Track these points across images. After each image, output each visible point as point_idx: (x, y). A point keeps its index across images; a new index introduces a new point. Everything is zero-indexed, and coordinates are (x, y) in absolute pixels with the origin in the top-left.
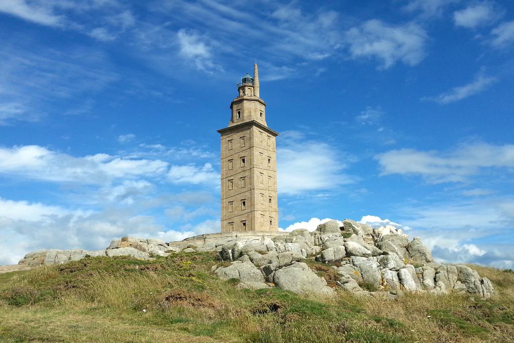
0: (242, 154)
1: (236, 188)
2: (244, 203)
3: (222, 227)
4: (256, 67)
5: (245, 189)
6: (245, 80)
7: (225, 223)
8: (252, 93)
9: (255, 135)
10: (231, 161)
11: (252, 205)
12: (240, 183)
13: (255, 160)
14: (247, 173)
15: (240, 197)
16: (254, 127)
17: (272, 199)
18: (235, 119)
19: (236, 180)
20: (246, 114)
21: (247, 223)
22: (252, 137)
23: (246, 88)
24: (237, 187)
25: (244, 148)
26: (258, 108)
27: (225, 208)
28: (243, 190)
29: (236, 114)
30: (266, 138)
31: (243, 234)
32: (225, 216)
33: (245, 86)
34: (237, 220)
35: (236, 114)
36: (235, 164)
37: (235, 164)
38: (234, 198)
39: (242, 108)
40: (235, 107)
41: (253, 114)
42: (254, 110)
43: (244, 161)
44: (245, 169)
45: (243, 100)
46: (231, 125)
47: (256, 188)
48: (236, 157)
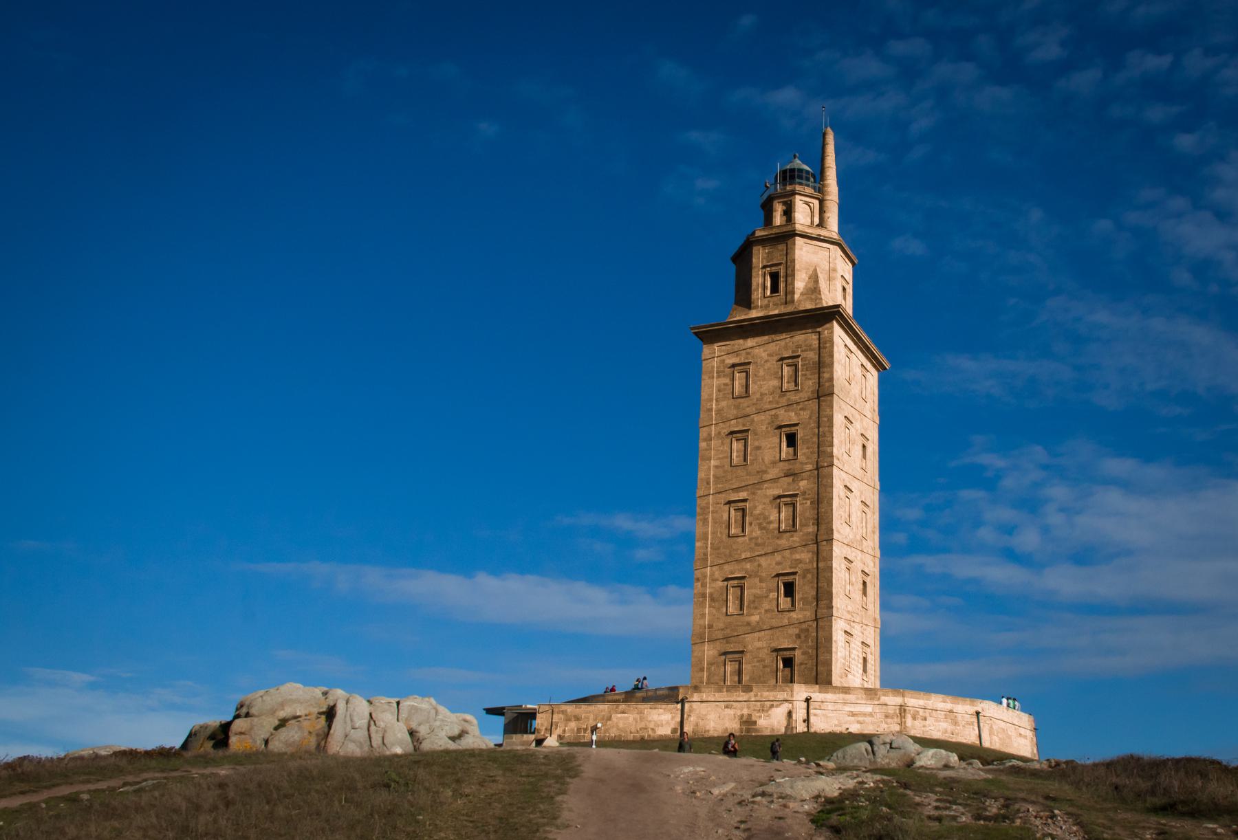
1: (757, 533)
2: (789, 590)
4: (830, 139)
5: (796, 538)
9: (836, 355)
11: (823, 597)
12: (773, 516)
13: (835, 441)
15: (770, 565)
16: (839, 335)
17: (868, 580)
18: (757, 295)
19: (760, 505)
20: (800, 284)
21: (798, 656)
22: (827, 360)
24: (762, 528)
25: (794, 397)
26: (839, 268)
27: (712, 600)
28: (784, 542)
29: (760, 281)
30: (858, 371)
31: (829, 696)
32: (710, 626)
33: (794, 193)
34: (758, 644)
36: (758, 448)
40: (760, 256)
41: (823, 284)
44: (796, 467)
45: (793, 234)
46: (741, 315)
47: (836, 535)
48: (761, 422)
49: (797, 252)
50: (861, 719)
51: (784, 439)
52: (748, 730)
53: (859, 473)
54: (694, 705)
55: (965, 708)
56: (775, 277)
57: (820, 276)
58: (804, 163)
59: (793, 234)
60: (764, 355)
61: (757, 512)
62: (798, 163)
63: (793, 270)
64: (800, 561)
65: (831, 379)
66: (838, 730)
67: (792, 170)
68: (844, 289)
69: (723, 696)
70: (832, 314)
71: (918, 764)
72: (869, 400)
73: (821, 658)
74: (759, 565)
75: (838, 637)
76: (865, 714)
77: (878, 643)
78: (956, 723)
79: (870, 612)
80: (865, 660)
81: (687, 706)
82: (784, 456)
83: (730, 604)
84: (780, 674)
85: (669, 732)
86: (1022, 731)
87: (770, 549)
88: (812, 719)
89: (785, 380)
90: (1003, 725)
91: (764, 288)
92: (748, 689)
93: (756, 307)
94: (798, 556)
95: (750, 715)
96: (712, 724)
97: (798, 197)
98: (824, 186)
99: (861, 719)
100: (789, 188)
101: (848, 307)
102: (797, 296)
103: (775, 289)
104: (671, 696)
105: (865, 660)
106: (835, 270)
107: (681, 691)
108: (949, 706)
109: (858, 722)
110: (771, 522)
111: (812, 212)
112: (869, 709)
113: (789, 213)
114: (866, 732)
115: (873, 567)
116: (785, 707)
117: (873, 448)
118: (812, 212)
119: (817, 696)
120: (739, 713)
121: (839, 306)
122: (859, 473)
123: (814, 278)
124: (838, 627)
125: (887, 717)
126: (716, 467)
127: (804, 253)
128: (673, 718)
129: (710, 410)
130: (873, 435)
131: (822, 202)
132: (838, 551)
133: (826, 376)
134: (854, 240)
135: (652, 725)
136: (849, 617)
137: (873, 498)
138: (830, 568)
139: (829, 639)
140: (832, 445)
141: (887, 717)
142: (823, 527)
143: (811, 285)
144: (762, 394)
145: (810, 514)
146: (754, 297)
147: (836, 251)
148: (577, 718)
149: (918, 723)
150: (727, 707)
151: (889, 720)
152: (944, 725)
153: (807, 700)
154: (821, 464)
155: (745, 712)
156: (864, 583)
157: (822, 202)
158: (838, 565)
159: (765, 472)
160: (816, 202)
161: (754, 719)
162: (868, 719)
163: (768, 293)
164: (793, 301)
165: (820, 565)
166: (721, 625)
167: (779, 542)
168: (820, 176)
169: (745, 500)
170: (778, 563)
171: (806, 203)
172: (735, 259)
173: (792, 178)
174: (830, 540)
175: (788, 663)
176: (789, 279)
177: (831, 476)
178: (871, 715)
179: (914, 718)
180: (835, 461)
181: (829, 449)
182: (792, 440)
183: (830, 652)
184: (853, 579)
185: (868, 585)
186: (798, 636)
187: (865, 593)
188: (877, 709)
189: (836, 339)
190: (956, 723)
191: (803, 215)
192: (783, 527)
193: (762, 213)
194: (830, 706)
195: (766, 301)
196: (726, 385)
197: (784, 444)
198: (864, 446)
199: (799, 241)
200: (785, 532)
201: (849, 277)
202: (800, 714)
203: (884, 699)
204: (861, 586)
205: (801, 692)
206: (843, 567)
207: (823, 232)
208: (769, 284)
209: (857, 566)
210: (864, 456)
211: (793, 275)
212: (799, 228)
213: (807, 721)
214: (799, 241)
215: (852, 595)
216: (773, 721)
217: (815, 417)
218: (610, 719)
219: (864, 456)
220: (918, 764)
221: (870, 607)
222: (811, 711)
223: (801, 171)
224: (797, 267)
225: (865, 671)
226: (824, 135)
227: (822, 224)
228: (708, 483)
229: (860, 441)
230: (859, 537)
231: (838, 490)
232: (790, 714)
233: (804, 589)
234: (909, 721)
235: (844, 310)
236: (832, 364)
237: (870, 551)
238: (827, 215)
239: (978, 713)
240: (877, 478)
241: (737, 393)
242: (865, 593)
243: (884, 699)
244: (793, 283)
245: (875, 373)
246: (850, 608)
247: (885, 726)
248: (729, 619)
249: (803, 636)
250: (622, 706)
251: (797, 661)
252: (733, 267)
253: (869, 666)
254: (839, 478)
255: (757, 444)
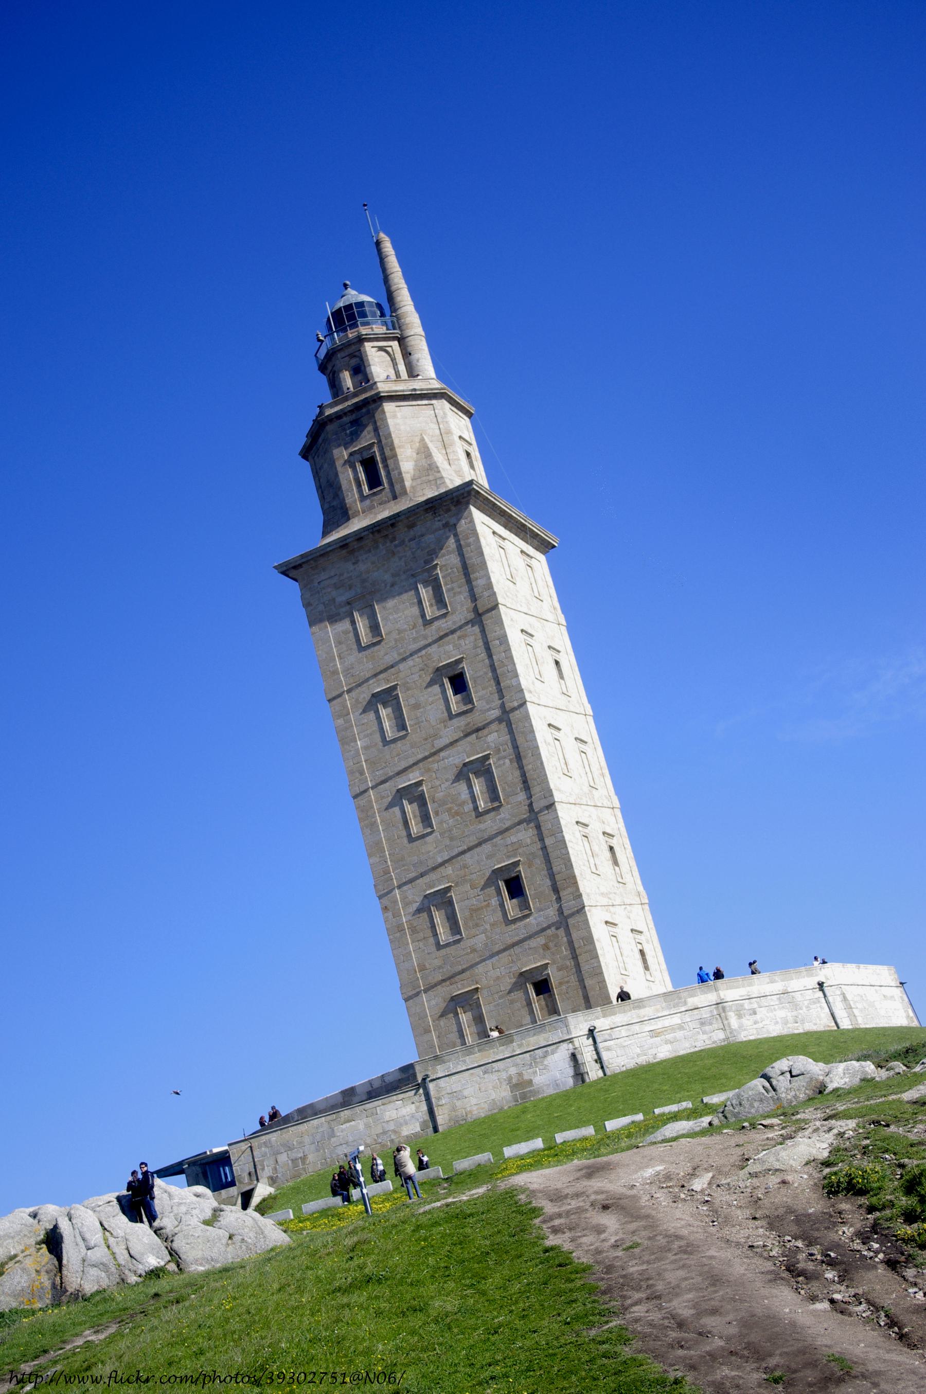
0: (446, 654)
2: (515, 887)
3: (420, 1029)
4: (388, 247)
5: (506, 816)
6: (347, 317)
7: (431, 1003)
8: (402, 368)
9: (486, 551)
10: (388, 697)
13: (520, 669)
14: (495, 737)
17: (614, 842)
18: (352, 496)
20: (407, 465)
23: (369, 348)
24: (453, 815)
25: (444, 625)
28: (490, 824)
30: (519, 562)
32: (422, 968)
33: (361, 340)
35: (350, 479)
36: (417, 706)
37: (417, 706)
38: (449, 870)
39: (383, 440)
41: (439, 458)
42: (432, 442)
43: (459, 684)
44: (476, 719)
45: (378, 399)
47: (557, 796)
49: (390, 422)
50: (669, 1037)
51: (448, 685)
52: (524, 1096)
53: (562, 702)
54: (442, 1082)
55: (802, 983)
56: (370, 466)
57: (430, 445)
58: (360, 293)
59: (378, 399)
60: (387, 577)
61: (440, 795)
62: (353, 296)
63: (393, 448)
64: (520, 844)
65: (489, 586)
66: (642, 1060)
67: (349, 307)
68: (468, 454)
69: (477, 1058)
70: (464, 496)
71: (831, 1087)
72: (545, 597)
73: (585, 968)
74: (465, 867)
75: (599, 932)
76: (672, 1029)
77: (651, 925)
78: (795, 1006)
79: (630, 886)
80: (642, 952)
81: (431, 1086)
82: (454, 708)
83: (440, 930)
84: (536, 1006)
85: (418, 1129)
86: (884, 990)
87: (473, 841)
88: (605, 1056)
89: (426, 604)
90: (860, 990)
91: (359, 485)
92: (505, 1038)
93: (356, 514)
94: (514, 839)
95: (520, 1074)
96: (474, 1101)
97: (368, 345)
98: (398, 318)
99: (669, 1037)
100: (351, 334)
101: (482, 479)
102: (408, 484)
103: (374, 481)
104: (406, 1079)
105: (642, 952)
106: (449, 432)
107: (418, 1068)
108: (778, 987)
109: (667, 1042)
110: (464, 803)
111: (393, 360)
112: (676, 1020)
113: (360, 370)
114: (682, 1053)
115: (616, 823)
116: (563, 1052)
117: (569, 660)
118: (393, 360)
119: (602, 1023)
120: (504, 1075)
121: (471, 482)
122: (562, 702)
123: (424, 452)
124: (595, 918)
125: (702, 1024)
126: (366, 748)
127: (400, 421)
128: (417, 1108)
129: (335, 672)
130: (563, 642)
131: (401, 340)
132: (566, 815)
133: (479, 583)
134: (462, 385)
135: (392, 1126)
136: (605, 901)
137: (588, 728)
138: (563, 842)
139: (589, 939)
140: (517, 676)
141: (702, 1024)
142: (536, 790)
143: (424, 463)
144: (400, 632)
145: (514, 776)
146: (348, 501)
147: (443, 406)
148: (289, 1148)
149: (747, 1021)
150: (485, 1073)
151: (707, 1028)
152: (781, 1014)
153: (591, 1033)
154: (509, 705)
155: (513, 1071)
156: (611, 848)
157: (401, 340)
158: (571, 835)
159: (436, 736)
160: (395, 344)
161: (526, 1077)
162: (679, 1034)
163: (365, 488)
164: (404, 492)
165: (548, 842)
166: (437, 962)
167: (482, 826)
168: (388, 307)
169: (419, 783)
170: (489, 857)
171: (381, 349)
172: (306, 453)
173: (352, 317)
174: (551, 806)
175: (543, 987)
176: (390, 462)
177: (527, 717)
178: (681, 1027)
179: (740, 1016)
180: (528, 696)
181: (514, 682)
182: (459, 684)
183: (596, 957)
184: (596, 848)
185: (616, 849)
186: (546, 947)
187: (616, 862)
188: (687, 1017)
189: (480, 528)
190: (795, 1006)
191: (380, 366)
192: (482, 805)
193: (323, 380)
194: (624, 1032)
195: (368, 502)
196: (346, 632)
197: (450, 692)
198: (557, 663)
199: (389, 407)
200: (487, 812)
201: (469, 435)
202: (587, 1056)
203: (693, 1001)
204: (608, 854)
205: (578, 1024)
206: (578, 835)
207: (417, 385)
208: (362, 476)
209: (595, 829)
210: (561, 676)
211: (395, 456)
212: (383, 388)
213: (599, 1060)
214: (389, 407)
215: (601, 870)
216: (553, 1073)
217: (480, 643)
218: (332, 1134)
219: (561, 676)
220: (831, 1087)
221: (628, 878)
222: (600, 1046)
223: (361, 304)
224: (396, 442)
225: (646, 968)
226: (378, 244)
227: (412, 373)
228: (362, 773)
229: (548, 659)
230: (586, 789)
231: (542, 735)
232: (574, 1056)
233: (534, 882)
234: (734, 1022)
235: (481, 486)
236: (484, 565)
237: (607, 803)
238: (414, 357)
239: (821, 985)
240: (585, 700)
241: (365, 640)
242: (616, 862)
243: (693, 1001)
244: (398, 467)
245: (542, 557)
246: (603, 890)
247: (705, 1037)
248: (443, 952)
249: (551, 945)
250: (345, 1114)
251: (554, 982)
252: (306, 466)
253: (649, 957)
254: (538, 717)
255: (412, 701)
